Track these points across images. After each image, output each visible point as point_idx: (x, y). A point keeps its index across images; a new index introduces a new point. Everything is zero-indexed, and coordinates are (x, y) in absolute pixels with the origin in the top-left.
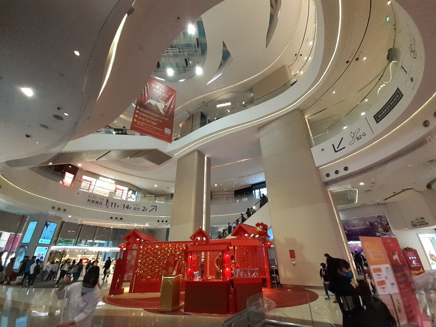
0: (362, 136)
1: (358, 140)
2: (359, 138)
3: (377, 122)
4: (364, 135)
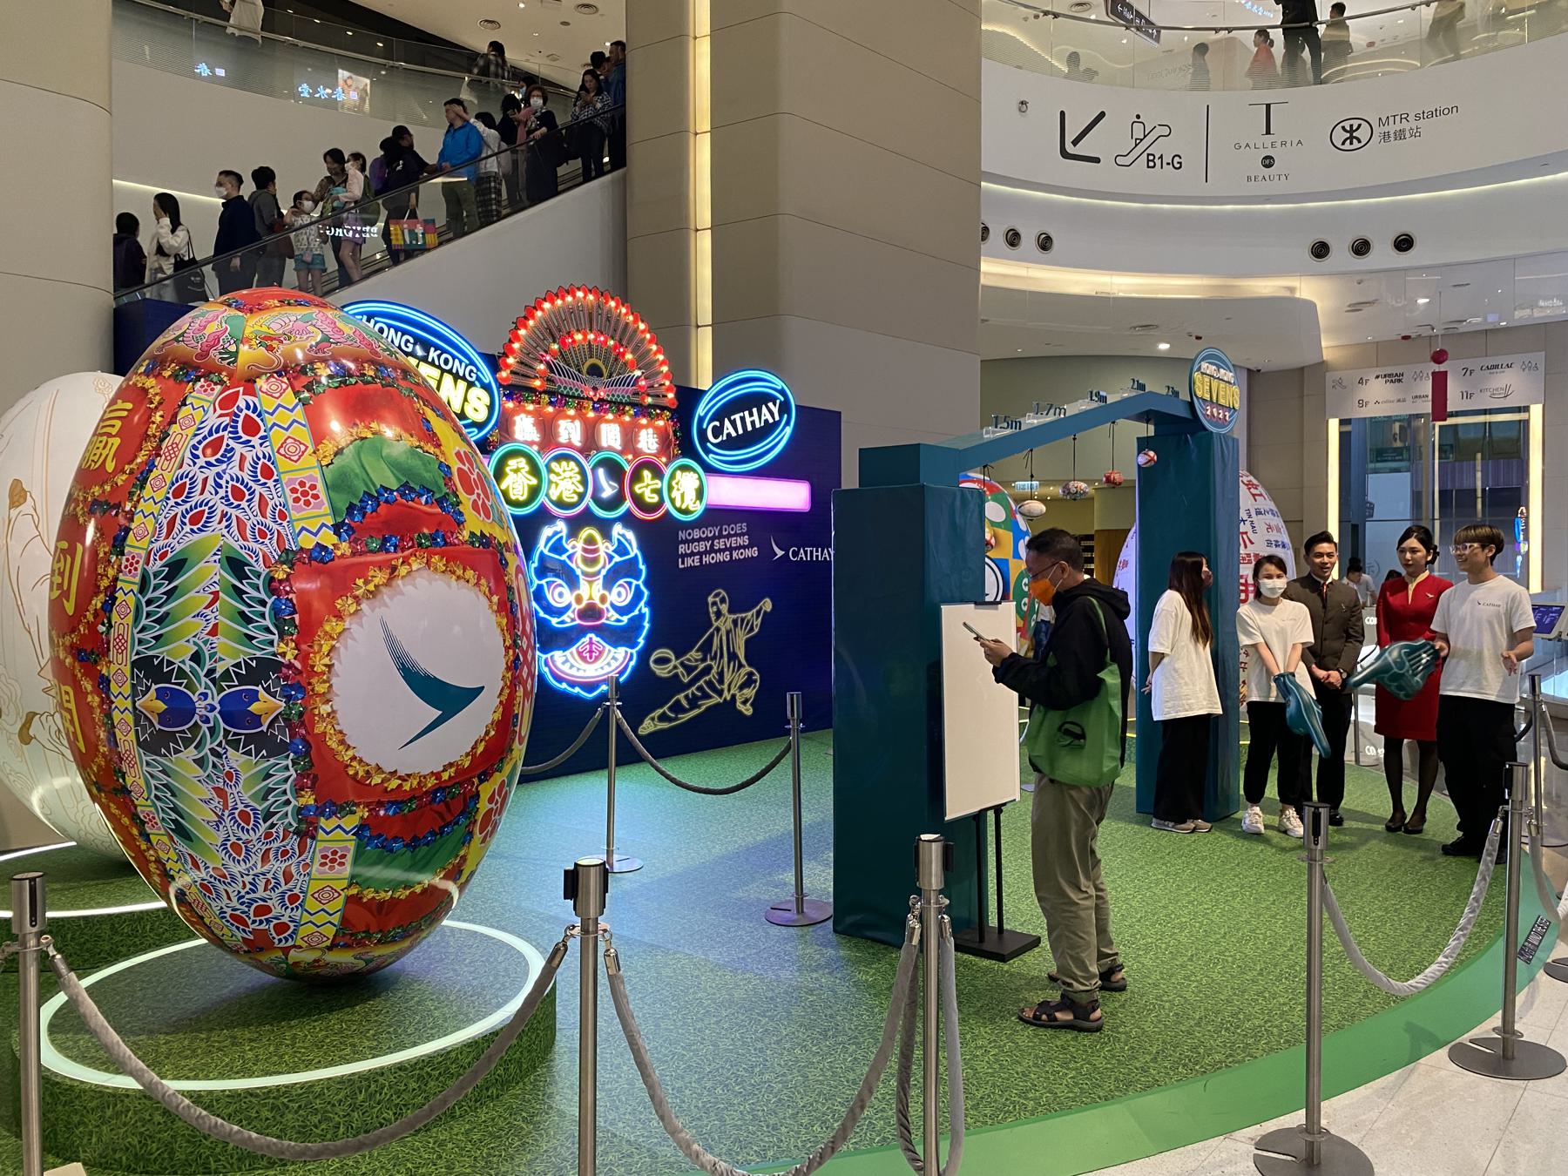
1: (1148, 167)
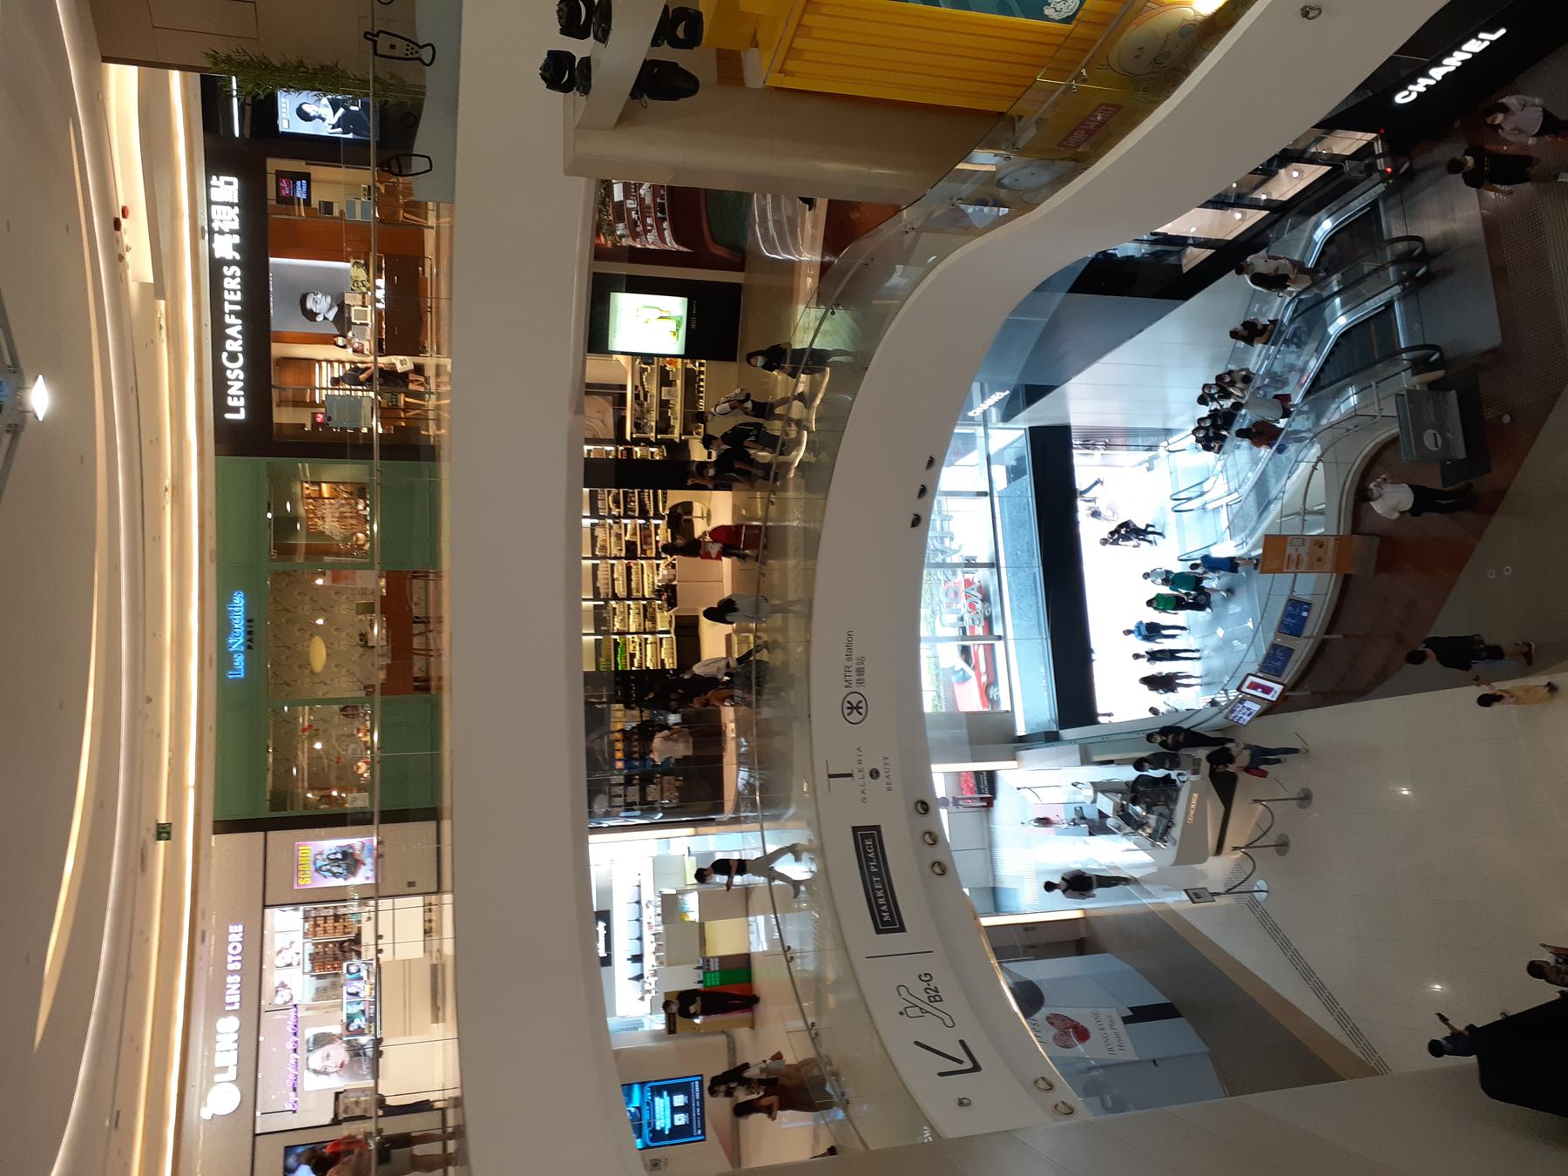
1: (941, 1000)
2: (933, 993)
4: (927, 977)
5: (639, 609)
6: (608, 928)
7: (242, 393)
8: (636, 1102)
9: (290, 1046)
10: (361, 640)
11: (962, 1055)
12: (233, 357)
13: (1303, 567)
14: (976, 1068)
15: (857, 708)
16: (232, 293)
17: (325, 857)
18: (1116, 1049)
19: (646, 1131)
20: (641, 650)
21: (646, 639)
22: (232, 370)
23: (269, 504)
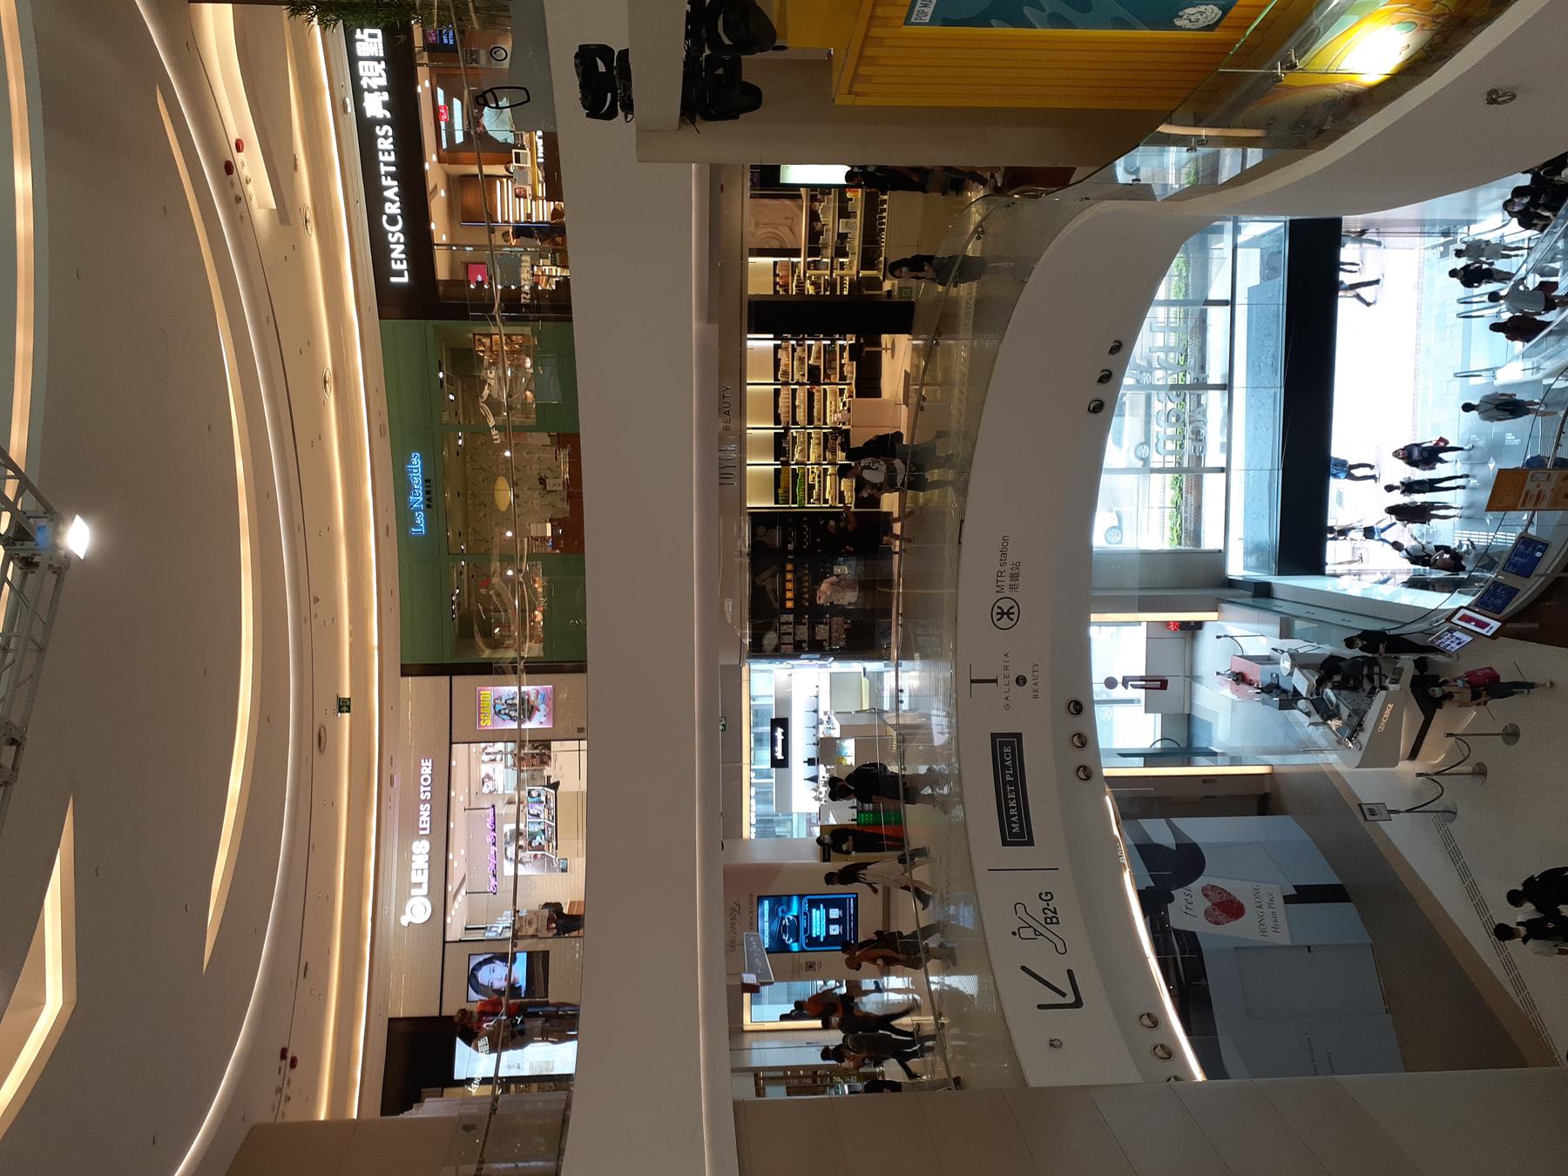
0: (1048, 905)
2: (1050, 914)
3: (1030, 843)
5: (819, 439)
6: (786, 734)
7: (403, 256)
8: (795, 911)
9: (489, 840)
10: (541, 483)
11: (1068, 989)
12: (392, 220)
13: (1544, 504)
14: (1078, 1003)
15: (1008, 613)
16: (386, 153)
17: (503, 702)
18: (1270, 930)
19: (803, 937)
20: (819, 482)
21: (827, 469)
22: (393, 233)
23: (440, 363)
